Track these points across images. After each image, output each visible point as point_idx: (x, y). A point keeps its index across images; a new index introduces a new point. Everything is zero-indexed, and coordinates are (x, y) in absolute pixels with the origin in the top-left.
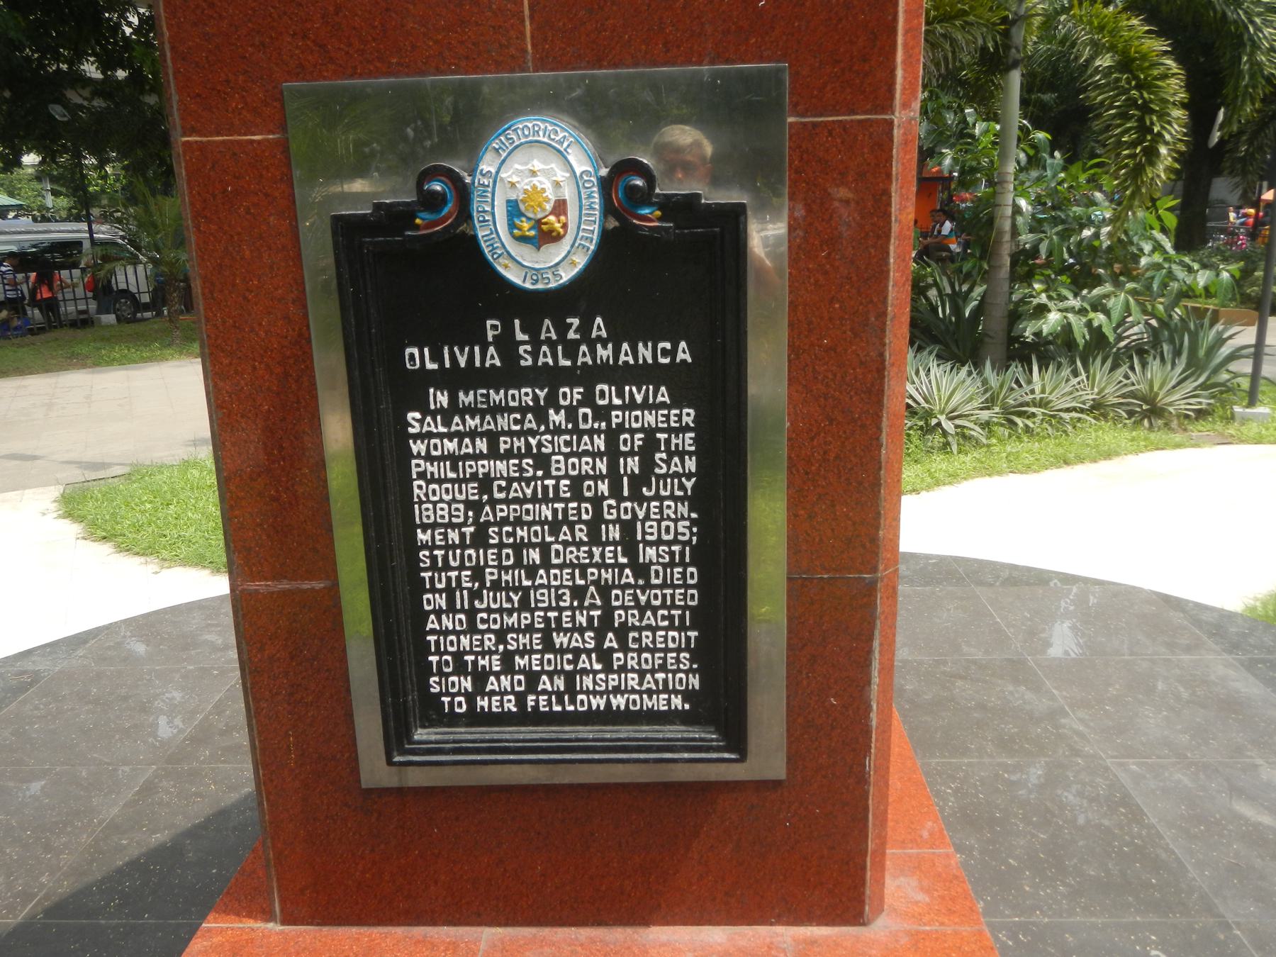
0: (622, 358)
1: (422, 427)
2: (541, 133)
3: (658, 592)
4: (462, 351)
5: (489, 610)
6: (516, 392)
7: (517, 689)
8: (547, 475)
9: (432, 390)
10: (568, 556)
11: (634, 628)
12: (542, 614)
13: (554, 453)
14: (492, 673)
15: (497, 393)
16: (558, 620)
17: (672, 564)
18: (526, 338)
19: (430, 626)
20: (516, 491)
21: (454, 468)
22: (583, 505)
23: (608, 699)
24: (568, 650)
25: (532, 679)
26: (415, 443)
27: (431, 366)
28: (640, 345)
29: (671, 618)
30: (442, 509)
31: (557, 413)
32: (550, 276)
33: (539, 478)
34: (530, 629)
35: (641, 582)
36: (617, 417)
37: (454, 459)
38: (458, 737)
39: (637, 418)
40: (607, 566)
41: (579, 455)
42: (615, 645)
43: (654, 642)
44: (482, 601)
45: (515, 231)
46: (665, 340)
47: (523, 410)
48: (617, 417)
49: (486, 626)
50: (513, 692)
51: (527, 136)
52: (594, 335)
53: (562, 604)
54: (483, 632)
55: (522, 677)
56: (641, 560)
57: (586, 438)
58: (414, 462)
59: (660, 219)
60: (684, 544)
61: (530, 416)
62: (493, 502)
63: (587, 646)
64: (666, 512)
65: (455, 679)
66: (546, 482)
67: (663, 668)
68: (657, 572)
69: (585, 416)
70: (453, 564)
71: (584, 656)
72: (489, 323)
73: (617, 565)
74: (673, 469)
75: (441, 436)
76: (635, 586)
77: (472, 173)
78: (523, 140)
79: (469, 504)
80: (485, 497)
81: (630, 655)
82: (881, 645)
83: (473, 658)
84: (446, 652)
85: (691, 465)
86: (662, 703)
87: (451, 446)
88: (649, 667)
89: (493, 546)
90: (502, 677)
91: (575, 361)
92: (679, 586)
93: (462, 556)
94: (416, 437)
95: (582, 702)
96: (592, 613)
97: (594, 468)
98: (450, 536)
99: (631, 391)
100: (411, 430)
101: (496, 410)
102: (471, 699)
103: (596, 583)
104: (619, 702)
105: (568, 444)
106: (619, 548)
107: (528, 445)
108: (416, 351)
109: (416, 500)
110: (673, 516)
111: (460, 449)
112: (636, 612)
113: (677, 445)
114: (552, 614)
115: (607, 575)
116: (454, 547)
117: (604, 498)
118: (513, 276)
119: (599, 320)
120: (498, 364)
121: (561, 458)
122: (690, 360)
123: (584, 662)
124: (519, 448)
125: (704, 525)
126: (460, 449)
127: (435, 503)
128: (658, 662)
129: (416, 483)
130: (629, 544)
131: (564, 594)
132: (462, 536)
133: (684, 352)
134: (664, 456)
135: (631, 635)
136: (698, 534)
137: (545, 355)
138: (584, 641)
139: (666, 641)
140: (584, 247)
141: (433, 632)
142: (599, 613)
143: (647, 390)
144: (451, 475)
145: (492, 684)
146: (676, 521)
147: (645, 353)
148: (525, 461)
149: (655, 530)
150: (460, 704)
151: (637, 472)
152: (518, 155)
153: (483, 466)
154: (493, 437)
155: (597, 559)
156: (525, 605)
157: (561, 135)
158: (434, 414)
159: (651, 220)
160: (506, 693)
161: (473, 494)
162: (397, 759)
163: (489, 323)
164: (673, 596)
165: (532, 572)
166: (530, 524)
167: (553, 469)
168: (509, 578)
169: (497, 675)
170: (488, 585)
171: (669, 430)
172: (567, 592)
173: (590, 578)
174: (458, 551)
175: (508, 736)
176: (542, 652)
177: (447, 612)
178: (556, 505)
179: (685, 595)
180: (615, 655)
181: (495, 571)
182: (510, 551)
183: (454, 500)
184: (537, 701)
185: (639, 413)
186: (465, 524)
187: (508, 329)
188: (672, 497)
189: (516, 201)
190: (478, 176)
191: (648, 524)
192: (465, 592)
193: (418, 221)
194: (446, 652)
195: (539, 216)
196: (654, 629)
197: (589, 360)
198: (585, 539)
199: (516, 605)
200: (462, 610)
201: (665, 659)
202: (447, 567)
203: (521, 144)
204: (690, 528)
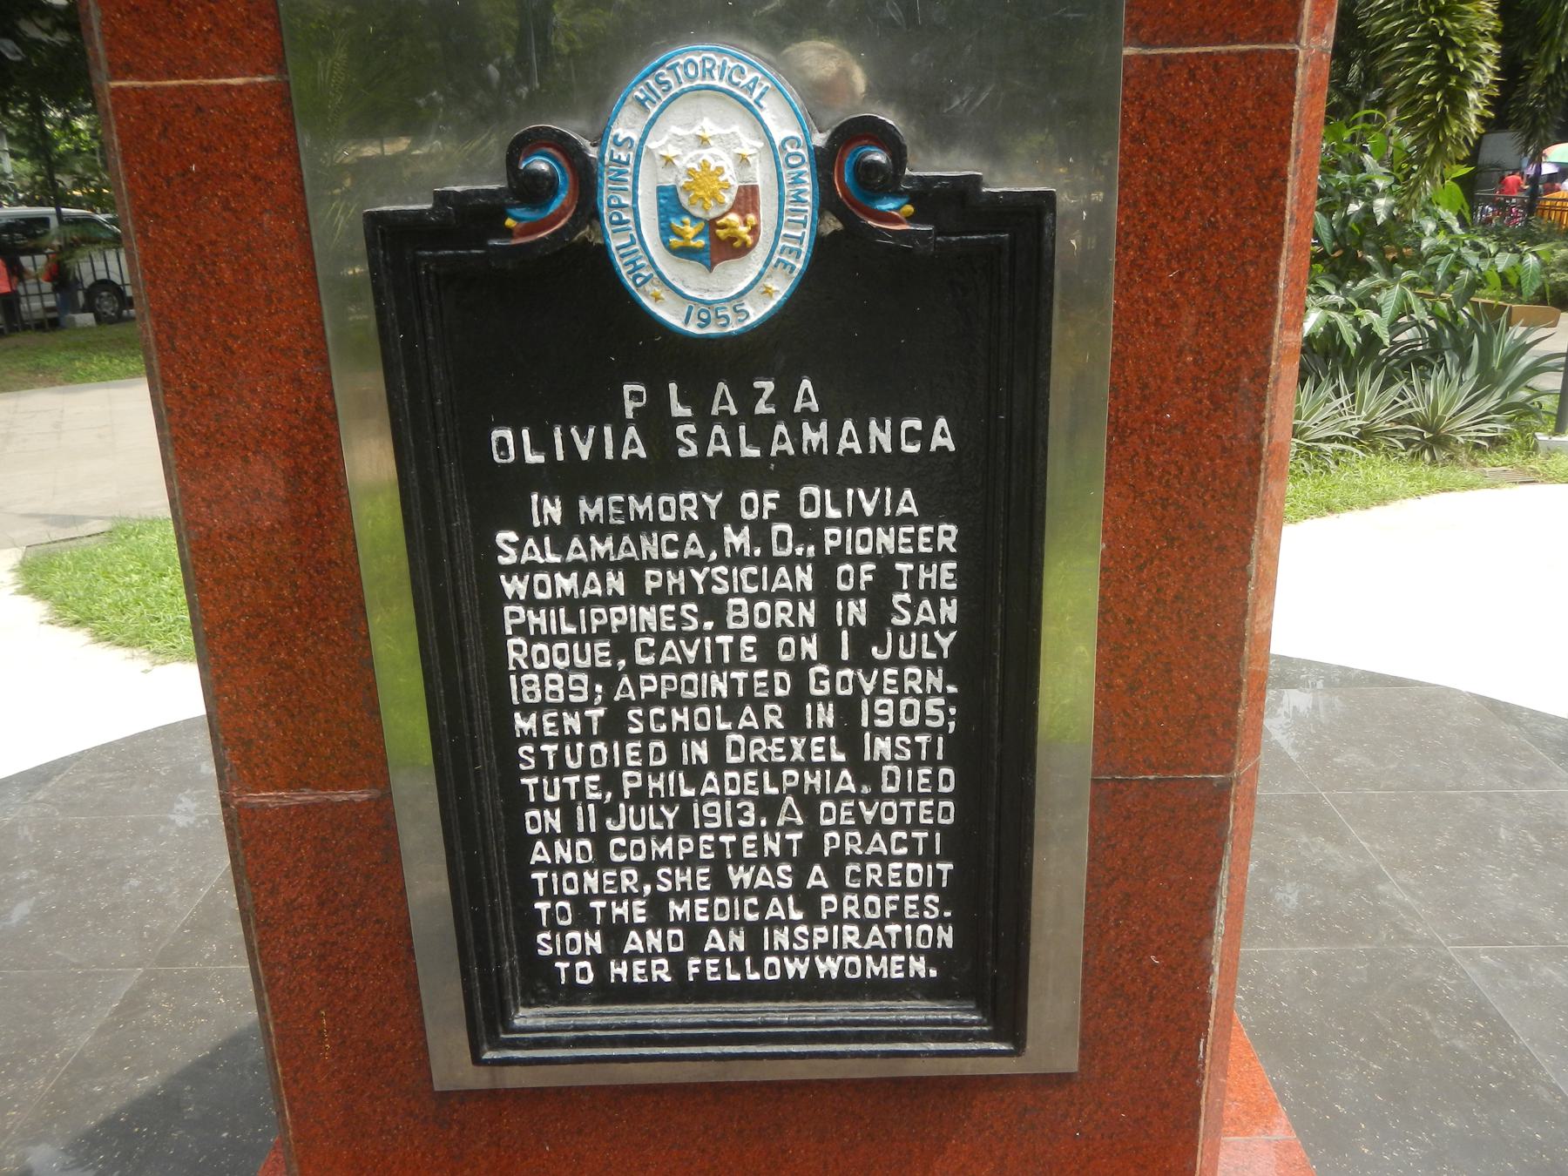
0: (844, 444)
1: (520, 555)
2: (716, 73)
3: (893, 804)
4: (583, 434)
5: (628, 833)
6: (672, 499)
7: (672, 949)
8: (721, 628)
9: (535, 497)
10: (753, 752)
11: (854, 858)
12: (711, 838)
13: (731, 594)
14: (633, 925)
15: (641, 500)
16: (737, 847)
17: (916, 763)
18: (688, 412)
19: (536, 858)
21: (573, 619)
22: (777, 674)
23: (812, 963)
24: (751, 892)
25: (696, 934)
26: (509, 580)
27: (533, 458)
28: (873, 423)
29: (911, 843)
30: (554, 682)
31: (737, 531)
32: (729, 313)
33: (708, 633)
34: (692, 860)
35: (866, 790)
36: (833, 537)
37: (572, 605)
38: (580, 1021)
39: (864, 539)
40: (813, 767)
41: (772, 597)
42: (824, 883)
43: (884, 878)
44: (617, 819)
45: (673, 240)
46: (913, 415)
47: (683, 527)
48: (833, 537)
49: (623, 858)
50: (666, 953)
51: (692, 79)
52: (798, 407)
53: (742, 823)
54: (618, 867)
55: (680, 932)
56: (867, 757)
57: (783, 571)
58: (508, 609)
59: (911, 219)
60: (935, 732)
61: (693, 537)
62: (634, 671)
63: (781, 885)
64: (908, 684)
65: (576, 935)
66: (720, 639)
67: (898, 917)
68: (891, 775)
69: (782, 535)
70: (571, 764)
71: (775, 901)
72: (628, 388)
73: (829, 763)
74: (921, 617)
75: (551, 568)
76: (857, 796)
77: (599, 140)
78: (686, 85)
79: (595, 674)
80: (622, 663)
81: (847, 898)
82: (1231, 877)
83: (603, 904)
84: (562, 896)
85: (950, 611)
86: (894, 967)
87: (567, 584)
88: (877, 916)
89: (635, 737)
90: (649, 933)
91: (766, 450)
92: (926, 796)
93: (586, 751)
94: (509, 571)
95: (772, 967)
96: (788, 836)
97: (794, 618)
98: (566, 723)
99: (856, 496)
100: (502, 560)
101: (639, 528)
102: (600, 963)
103: (796, 792)
104: (829, 967)
105: (754, 579)
106: (833, 739)
107: (690, 581)
108: (508, 434)
109: (512, 668)
110: (919, 691)
111: (581, 588)
112: (857, 834)
113: (928, 581)
114: (727, 839)
115: (813, 780)
116: (573, 739)
117: (810, 663)
118: (669, 313)
119: (806, 384)
120: (643, 455)
121: (743, 602)
122: (952, 448)
123: (775, 909)
124: (676, 587)
125: (968, 704)
126: (581, 588)
127: (542, 673)
128: (889, 908)
129: (511, 642)
130: (849, 732)
131: (746, 808)
132: (586, 722)
133: (943, 434)
134: (907, 598)
135: (849, 868)
136: (956, 718)
137: (718, 441)
138: (776, 878)
139: (903, 878)
140: (786, 265)
141: (541, 866)
142: (800, 836)
143: (883, 495)
144: (568, 629)
145: (633, 942)
146: (923, 698)
147: (880, 436)
148: (685, 607)
149: (890, 712)
150: (584, 972)
151: (863, 622)
152: (677, 110)
153: (618, 615)
154: (634, 570)
155: (798, 755)
156: (684, 824)
157: (750, 76)
158: (539, 534)
159: (897, 221)
160: (655, 954)
161: (602, 659)
162: (489, 1055)
163: (628, 388)
164: (915, 811)
165: (695, 775)
166: (692, 704)
167: (729, 619)
168: (660, 785)
169: (641, 929)
170: (627, 795)
171: (916, 558)
172: (751, 805)
173: (786, 784)
174: (580, 746)
175: (659, 1020)
176: (711, 895)
177: (563, 837)
178: (734, 675)
179: (934, 809)
180: (825, 899)
181: (638, 775)
182: (661, 744)
183: (573, 667)
184: (703, 967)
185: (868, 531)
186: (590, 704)
187: (659, 401)
188: (918, 661)
189: (674, 188)
190: (610, 146)
191: (879, 702)
192: (591, 807)
193: (510, 222)
194: (562, 896)
195: (713, 214)
196: (885, 860)
197: (789, 447)
198: (780, 726)
199: (671, 826)
200: (587, 834)
201: (901, 904)
203: (683, 92)
204: (945, 709)
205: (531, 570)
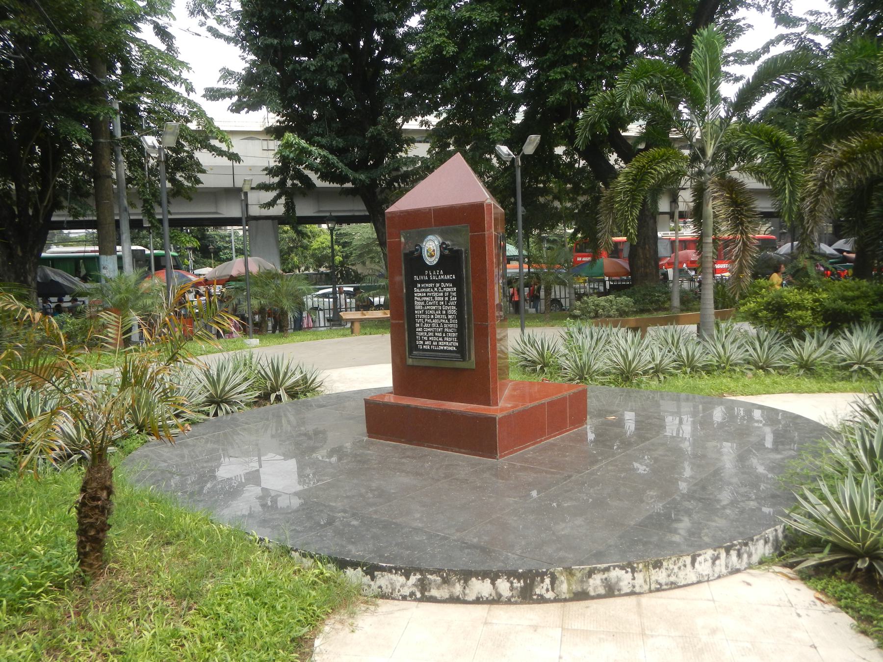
20: (430, 303)
25: (432, 342)
37: (421, 297)
130: (447, 315)
205: (418, 293)
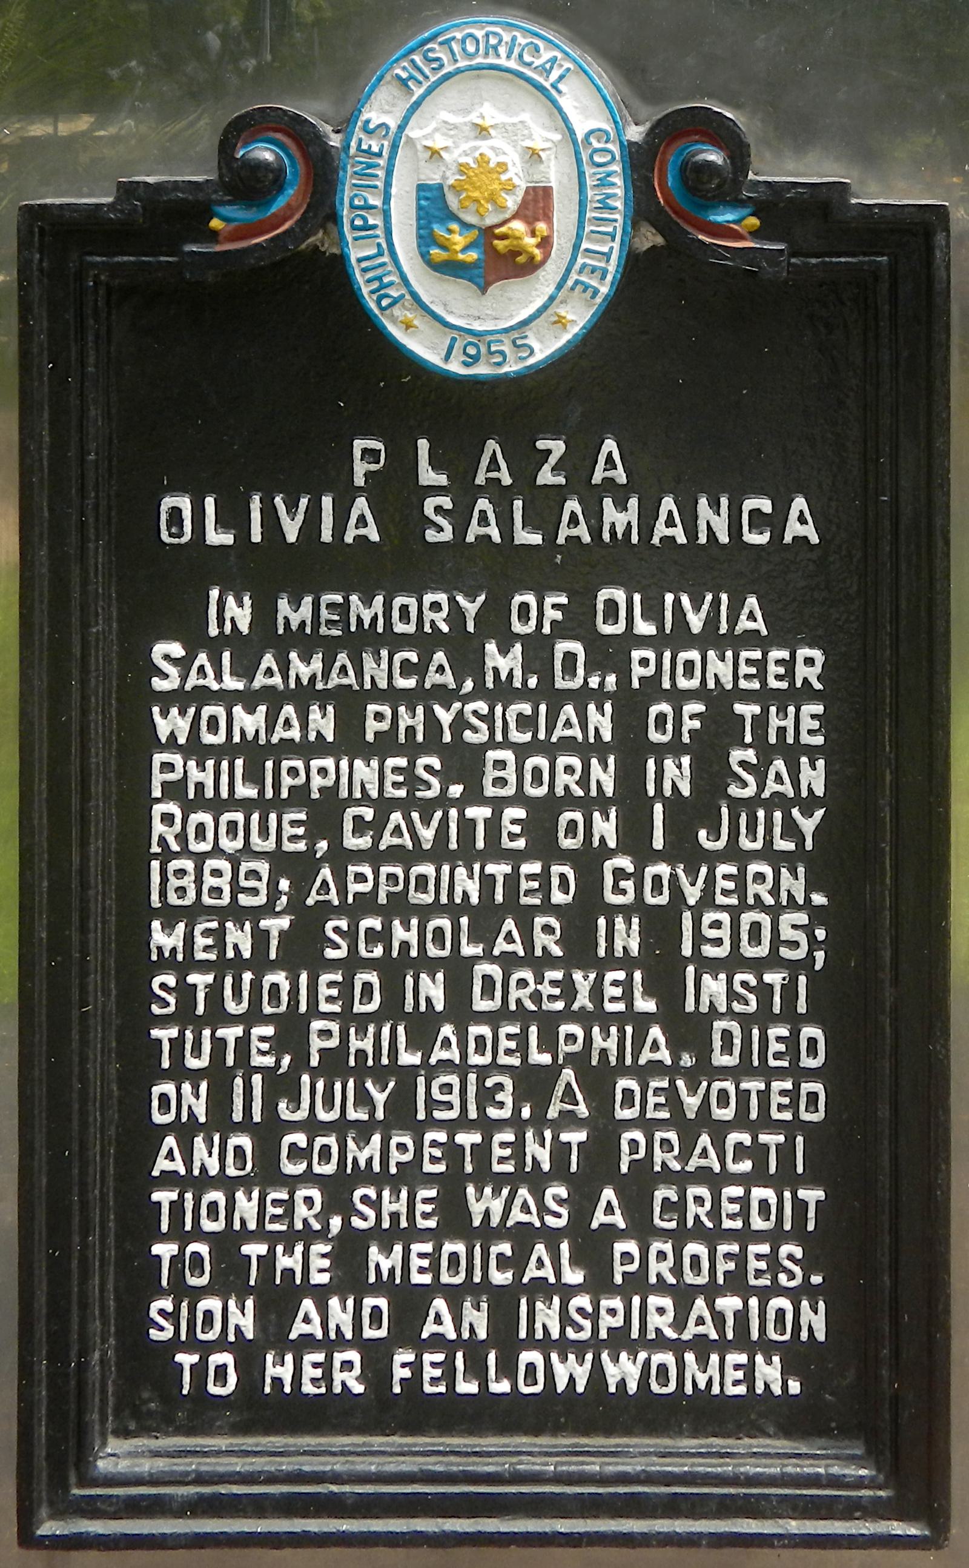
21: (254, 775)
25: (409, 1305)
34: (410, 1175)
37: (255, 754)
47: (426, 641)
60: (794, 967)
76: (673, 1071)
85: (814, 778)
101: (361, 641)
104: (623, 1370)
114: (467, 1139)
130: (662, 965)
153: (322, 772)
171: (764, 696)
202: (217, 1015)
